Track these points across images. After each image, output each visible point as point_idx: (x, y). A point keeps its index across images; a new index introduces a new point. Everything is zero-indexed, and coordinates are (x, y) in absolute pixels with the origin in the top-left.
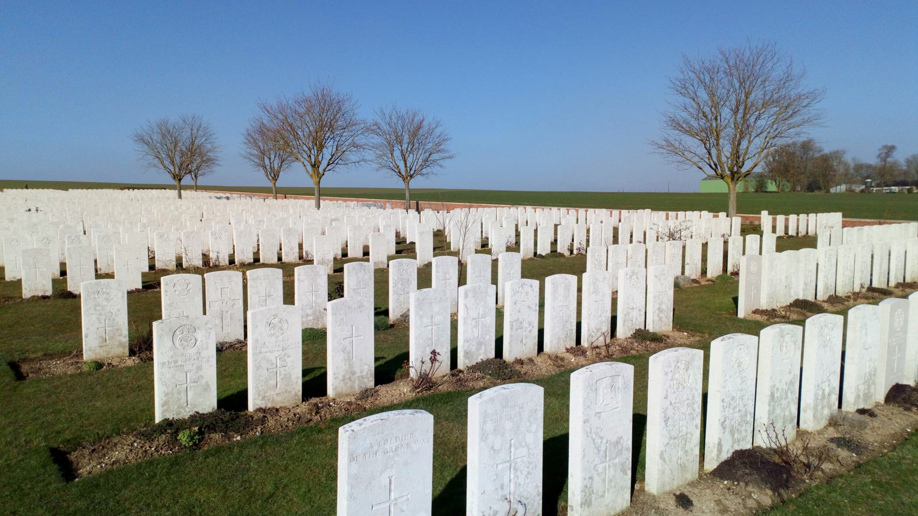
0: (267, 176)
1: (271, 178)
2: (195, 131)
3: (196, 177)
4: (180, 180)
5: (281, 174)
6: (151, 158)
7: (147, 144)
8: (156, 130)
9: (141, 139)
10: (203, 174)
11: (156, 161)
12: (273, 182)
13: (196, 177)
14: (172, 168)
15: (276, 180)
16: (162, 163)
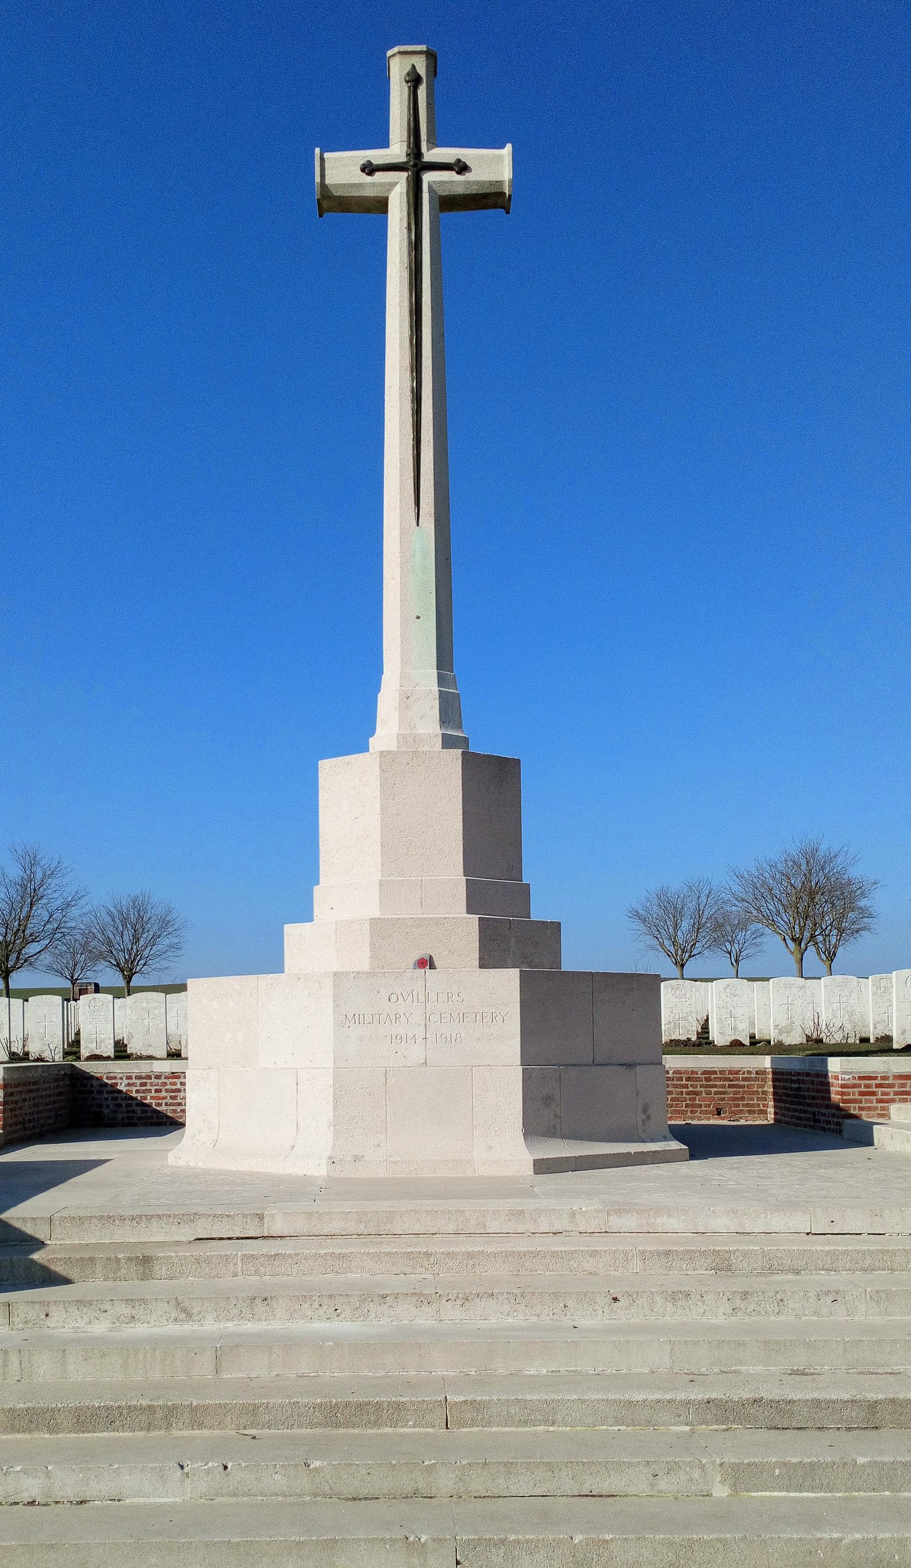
0: (819, 954)
1: (825, 958)
2: (703, 898)
3: (737, 961)
4: (683, 966)
5: (840, 951)
6: (650, 940)
7: (644, 921)
8: (655, 901)
9: (637, 915)
10: (748, 956)
11: (655, 942)
12: (828, 963)
13: (737, 961)
14: (672, 949)
15: (832, 960)
16: (662, 945)
